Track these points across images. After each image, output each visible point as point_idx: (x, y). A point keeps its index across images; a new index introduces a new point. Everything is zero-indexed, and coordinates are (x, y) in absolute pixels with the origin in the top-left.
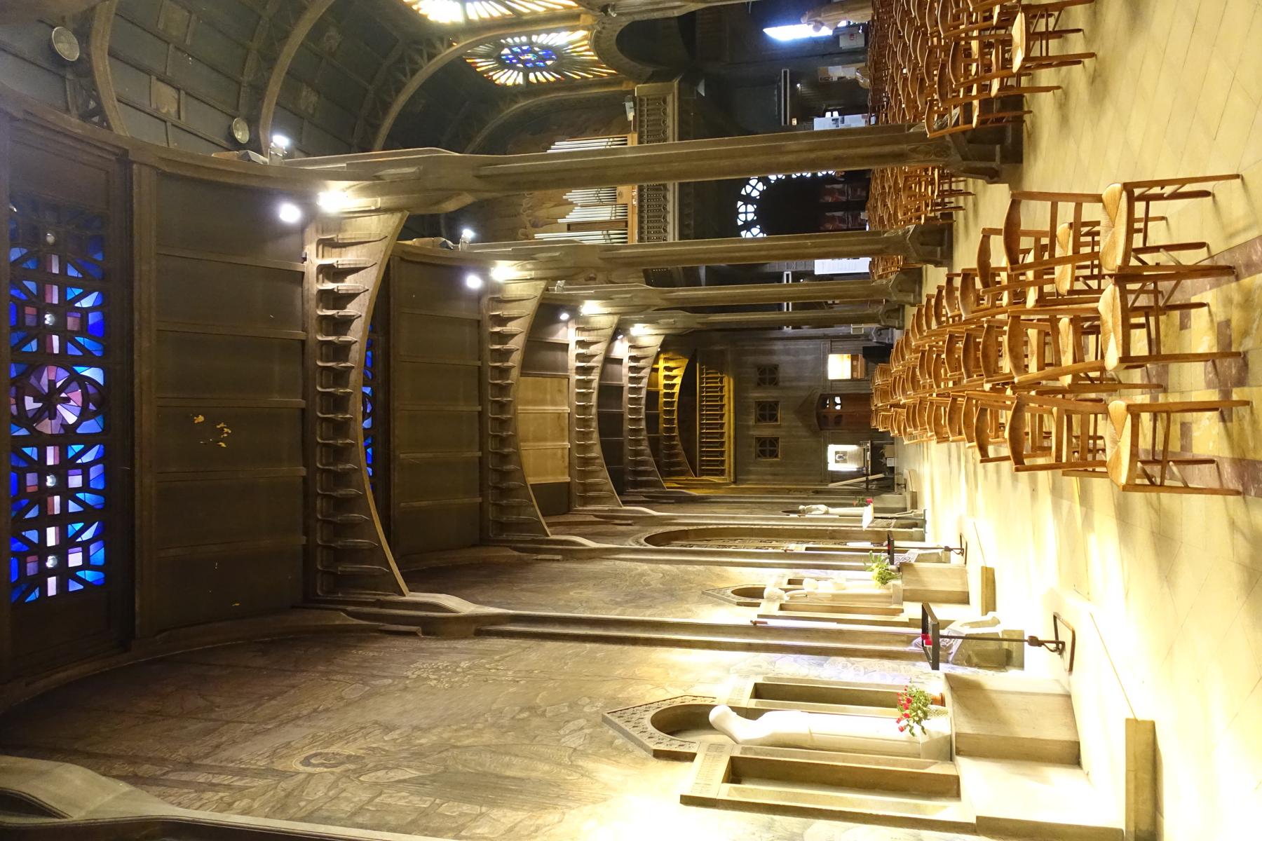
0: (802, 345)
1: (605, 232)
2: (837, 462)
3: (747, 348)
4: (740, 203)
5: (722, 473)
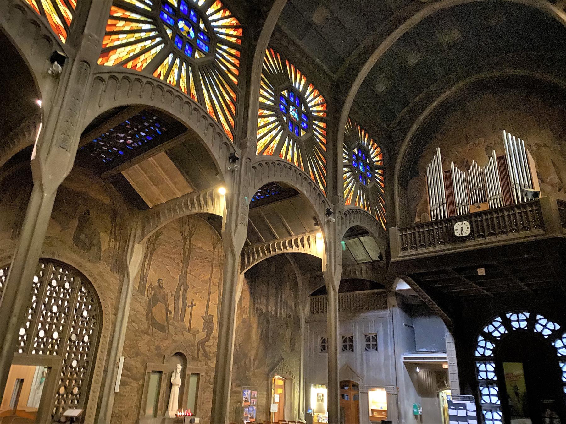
0: (392, 370)
1: (445, 201)
2: (318, 394)
3: (388, 326)
4: (528, 314)
5: (312, 313)
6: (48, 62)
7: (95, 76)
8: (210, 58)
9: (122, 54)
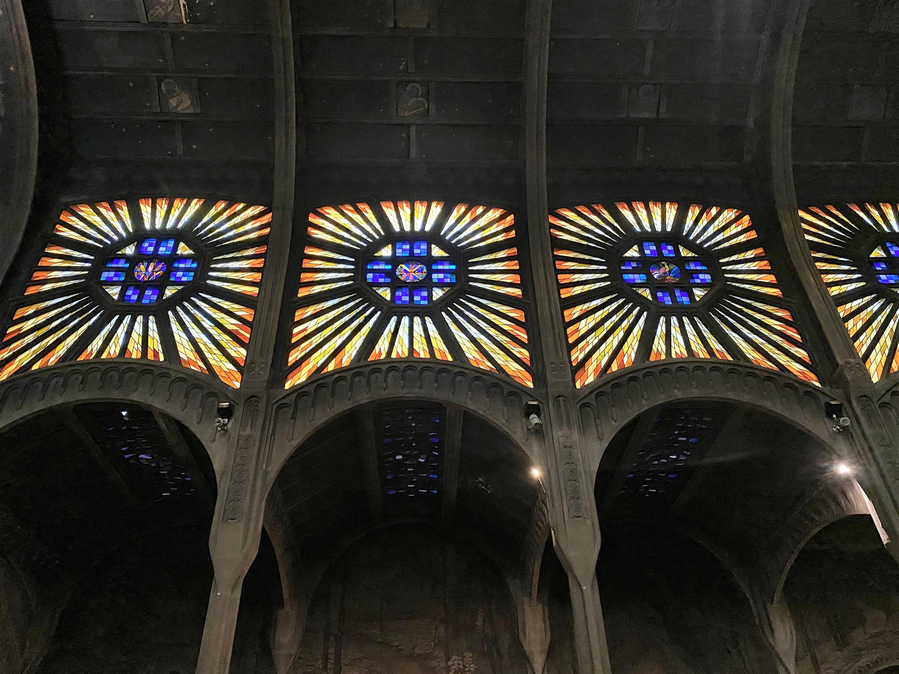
6: (524, 419)
7: (579, 405)
8: (718, 287)
9: (601, 358)
